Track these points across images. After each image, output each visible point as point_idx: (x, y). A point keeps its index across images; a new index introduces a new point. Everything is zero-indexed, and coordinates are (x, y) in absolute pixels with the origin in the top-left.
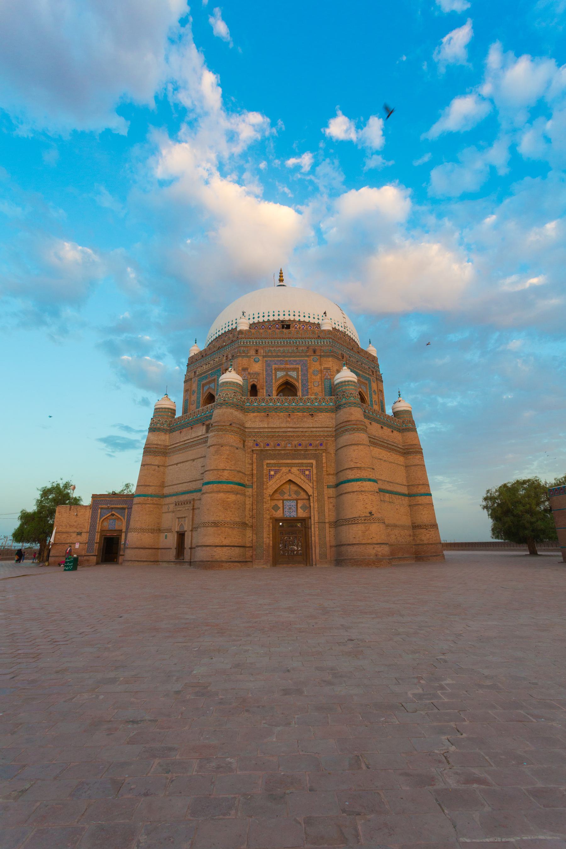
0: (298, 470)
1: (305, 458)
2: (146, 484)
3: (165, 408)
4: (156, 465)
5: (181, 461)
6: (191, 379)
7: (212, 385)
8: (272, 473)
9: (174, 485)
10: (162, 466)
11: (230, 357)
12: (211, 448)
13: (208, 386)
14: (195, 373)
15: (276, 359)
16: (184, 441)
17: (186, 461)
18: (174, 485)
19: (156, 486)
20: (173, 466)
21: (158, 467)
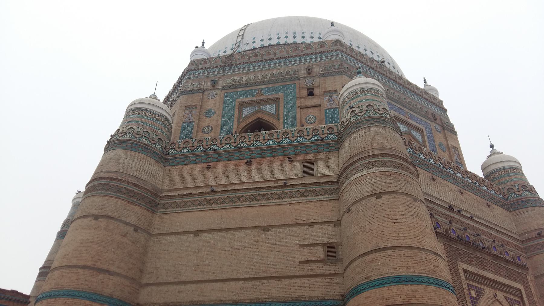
0: (506, 298)
1: (509, 277)
2: (99, 265)
3: (160, 115)
4: (132, 225)
5: (215, 227)
6: (203, 91)
7: (270, 108)
8: (473, 294)
9: (185, 283)
10: (144, 230)
11: (317, 70)
12: (385, 198)
13: (255, 108)
14: (214, 83)
15: (393, 103)
16: (225, 185)
17: (235, 229)
18: (185, 283)
19: (126, 277)
20: (186, 236)
21: (136, 230)
